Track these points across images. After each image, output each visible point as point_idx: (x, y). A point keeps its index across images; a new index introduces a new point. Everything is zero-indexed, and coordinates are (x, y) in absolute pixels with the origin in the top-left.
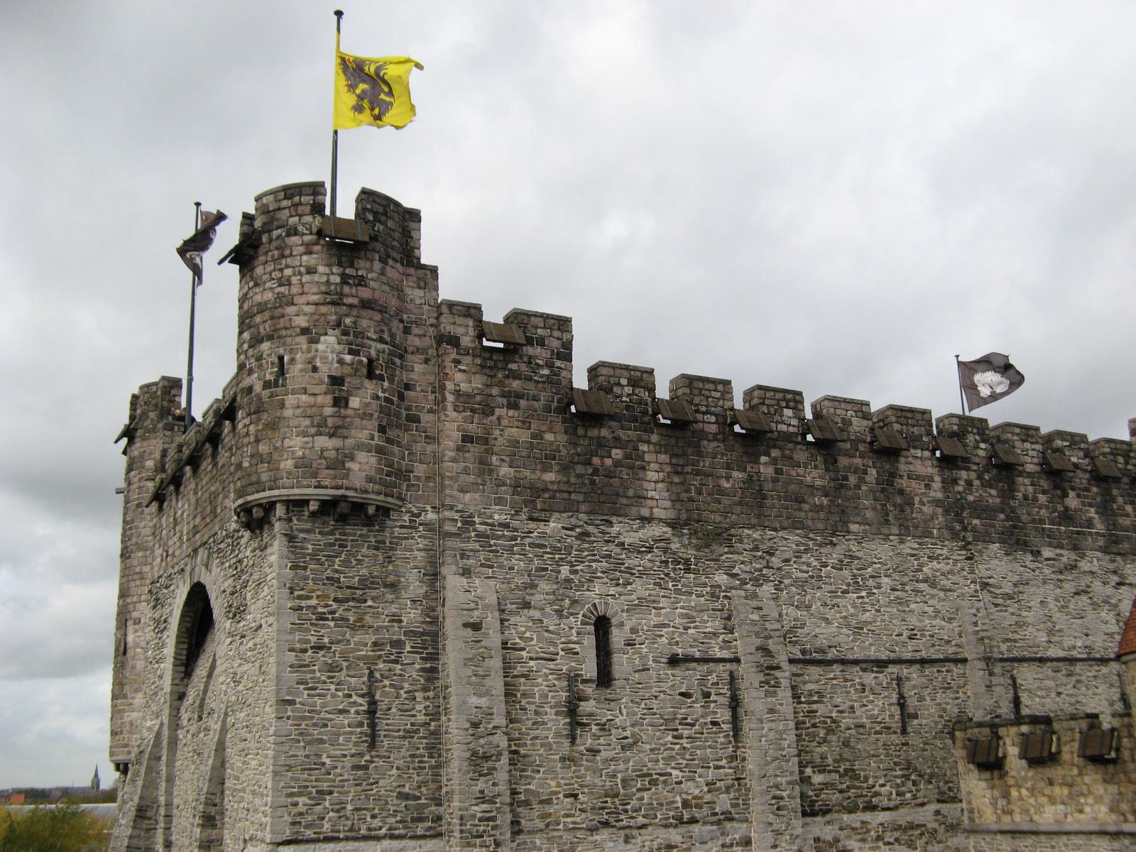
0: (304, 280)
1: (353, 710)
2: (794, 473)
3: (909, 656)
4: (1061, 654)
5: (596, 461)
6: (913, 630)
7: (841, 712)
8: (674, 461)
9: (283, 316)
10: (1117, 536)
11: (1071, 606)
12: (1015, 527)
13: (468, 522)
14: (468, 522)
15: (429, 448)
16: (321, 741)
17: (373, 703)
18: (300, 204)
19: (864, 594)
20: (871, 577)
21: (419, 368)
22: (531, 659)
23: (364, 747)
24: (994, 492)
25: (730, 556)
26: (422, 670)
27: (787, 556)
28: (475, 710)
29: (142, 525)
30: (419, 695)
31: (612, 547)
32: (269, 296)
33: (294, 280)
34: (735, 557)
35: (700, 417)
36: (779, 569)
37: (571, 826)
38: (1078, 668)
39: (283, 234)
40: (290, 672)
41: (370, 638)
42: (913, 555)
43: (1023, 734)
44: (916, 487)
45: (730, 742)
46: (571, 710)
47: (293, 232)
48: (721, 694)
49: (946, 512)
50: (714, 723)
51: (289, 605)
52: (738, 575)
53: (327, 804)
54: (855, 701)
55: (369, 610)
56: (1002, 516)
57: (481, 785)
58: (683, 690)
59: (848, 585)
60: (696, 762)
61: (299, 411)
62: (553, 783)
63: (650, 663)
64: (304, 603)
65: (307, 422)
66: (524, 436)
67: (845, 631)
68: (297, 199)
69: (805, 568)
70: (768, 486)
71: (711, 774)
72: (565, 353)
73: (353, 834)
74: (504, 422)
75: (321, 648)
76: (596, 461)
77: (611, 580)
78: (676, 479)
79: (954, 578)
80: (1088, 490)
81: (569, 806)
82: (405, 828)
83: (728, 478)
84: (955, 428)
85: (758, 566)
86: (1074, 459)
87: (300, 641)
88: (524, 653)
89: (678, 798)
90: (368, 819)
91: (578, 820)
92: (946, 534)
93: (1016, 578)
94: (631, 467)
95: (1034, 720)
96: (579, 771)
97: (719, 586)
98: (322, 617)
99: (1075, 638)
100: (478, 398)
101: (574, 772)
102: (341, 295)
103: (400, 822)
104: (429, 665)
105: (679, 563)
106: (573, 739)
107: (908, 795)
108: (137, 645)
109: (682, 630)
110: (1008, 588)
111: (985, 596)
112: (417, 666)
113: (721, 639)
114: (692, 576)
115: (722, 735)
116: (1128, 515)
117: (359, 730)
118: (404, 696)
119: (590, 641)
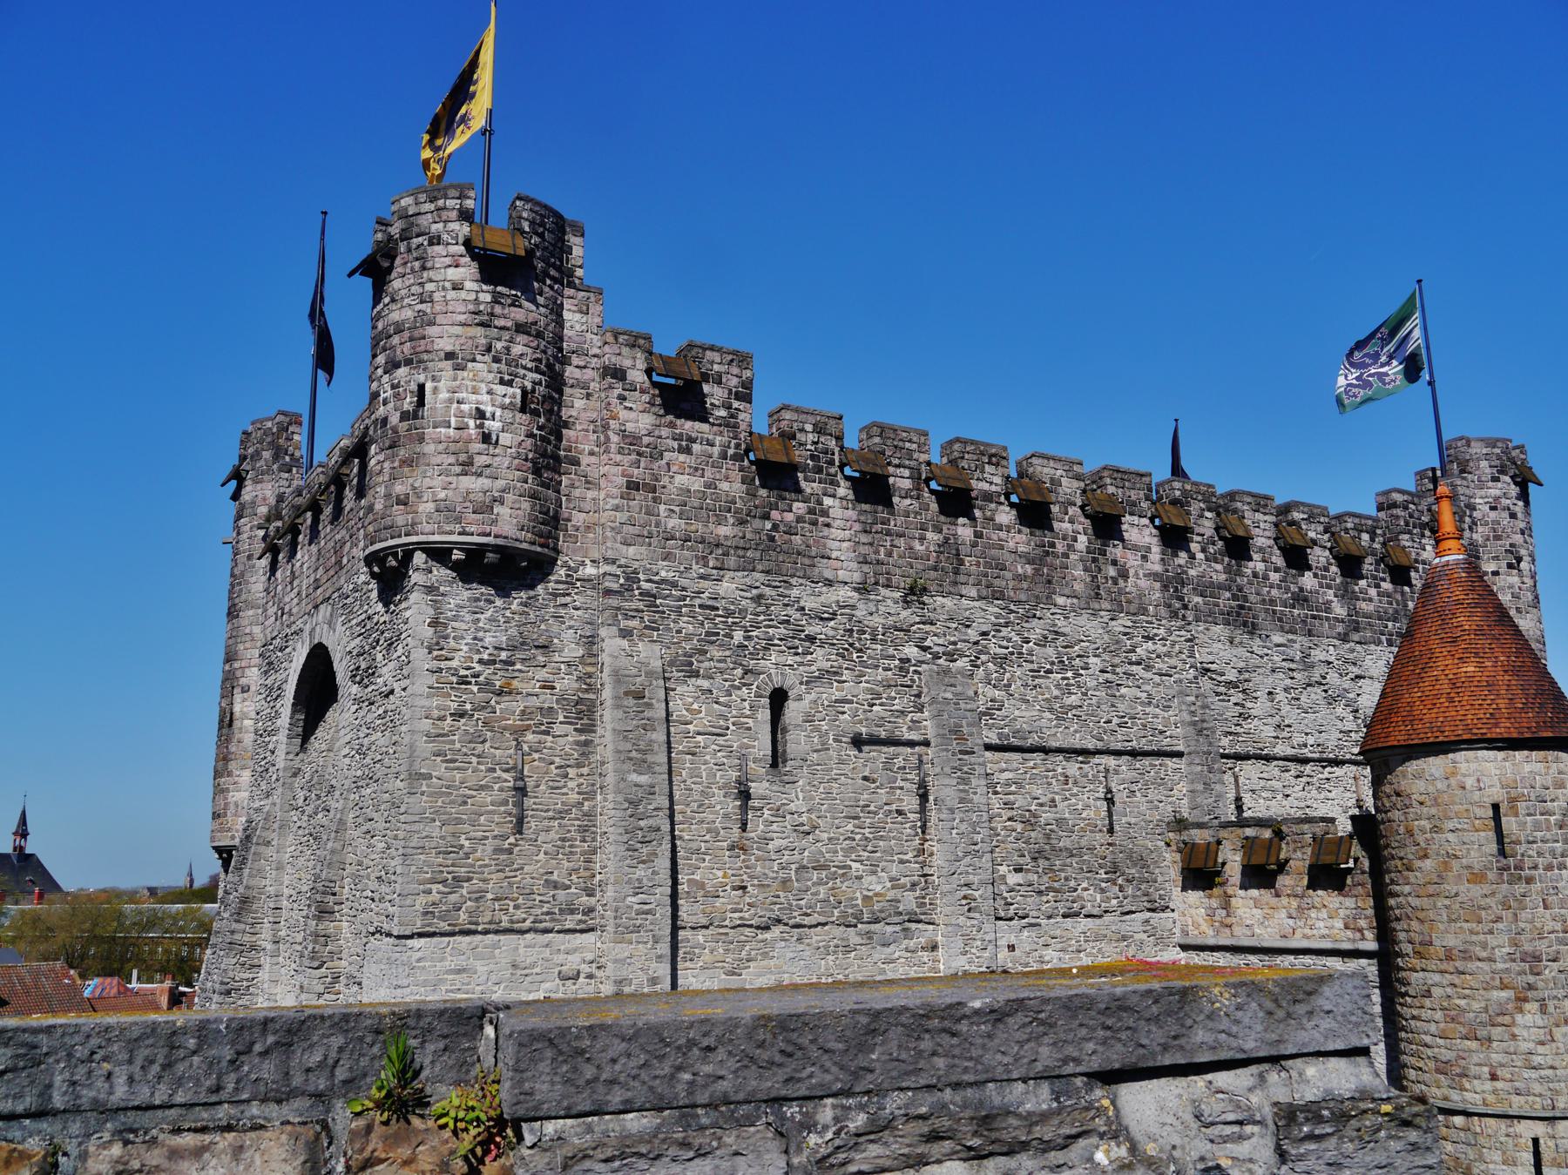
0: (448, 298)
1: (496, 787)
2: (995, 537)
3: (1119, 746)
4: (1290, 752)
5: (775, 514)
6: (1123, 717)
7: (1041, 805)
8: (862, 518)
9: (424, 338)
10: (1357, 622)
11: (1303, 698)
12: (1242, 607)
13: (632, 578)
15: (590, 494)
16: (459, 822)
18: (445, 208)
19: (1069, 674)
20: (1078, 656)
21: (579, 404)
22: (699, 734)
23: (508, 828)
24: (1219, 567)
25: (921, 626)
26: (577, 743)
27: (985, 628)
28: (634, 789)
30: (572, 772)
31: (790, 611)
32: (408, 314)
33: (437, 296)
34: (927, 628)
35: (891, 469)
36: (976, 643)
37: (739, 922)
38: (1308, 768)
39: (426, 243)
40: (426, 742)
41: (519, 706)
42: (1125, 634)
43: (1247, 838)
44: (1132, 561)
45: (917, 834)
47: (435, 240)
48: (907, 780)
49: (1165, 588)
50: (900, 812)
51: (427, 666)
52: (930, 648)
53: (464, 892)
54: (1057, 793)
55: (517, 674)
56: (1228, 595)
57: (640, 872)
58: (866, 774)
59: (1053, 663)
60: (878, 854)
61: (441, 447)
62: (720, 874)
63: (831, 741)
64: (443, 665)
65: (452, 459)
66: (697, 484)
67: (1047, 715)
68: (441, 203)
69: (1005, 643)
70: (964, 550)
71: (895, 869)
73: (493, 926)
74: (674, 469)
75: (462, 715)
76: (775, 514)
77: (789, 648)
78: (864, 538)
79: (1173, 662)
80: (1326, 569)
81: (737, 900)
82: (553, 920)
83: (922, 539)
84: (1178, 493)
85: (952, 639)
86: (1312, 535)
87: (438, 708)
88: (691, 727)
89: (858, 895)
90: (511, 910)
91: (747, 915)
92: (1163, 611)
93: (1242, 665)
95: (1260, 823)
96: (749, 860)
97: (908, 660)
98: (464, 681)
99: (1307, 734)
100: (646, 440)
101: (744, 861)
102: (492, 314)
103: (548, 913)
104: (583, 738)
105: (864, 633)
107: (1114, 902)
108: (245, 716)
109: (866, 707)
110: (1231, 676)
111: (1206, 684)
112: (570, 739)
113: (909, 718)
114: (879, 647)
115: (908, 825)
116: (1371, 600)
117: (502, 809)
118: (555, 771)
119: (765, 715)
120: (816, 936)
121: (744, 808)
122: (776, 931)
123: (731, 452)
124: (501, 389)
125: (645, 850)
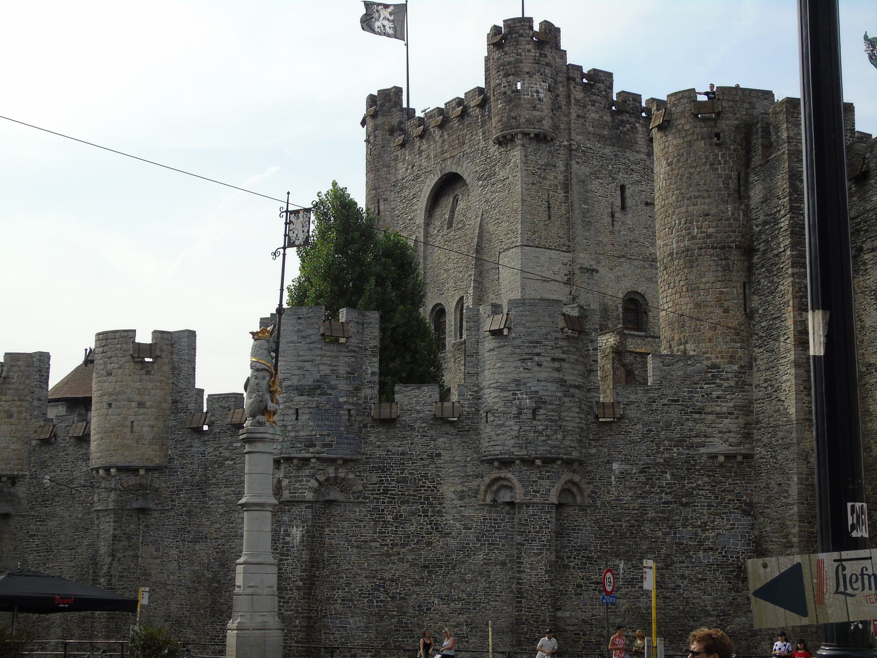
5: (621, 128)
14: (579, 146)
16: (534, 215)
17: (549, 204)
21: (561, 89)
23: (547, 219)
29: (386, 156)
32: (512, 59)
46: (613, 215)
47: (521, 36)
66: (596, 116)
72: (611, 87)
76: (621, 128)
94: (633, 132)
102: (539, 60)
106: (613, 226)
119: (619, 192)
120: (635, 263)
121: (613, 221)
122: (622, 260)
123: (607, 106)
124: (543, 84)
125: (587, 227)
